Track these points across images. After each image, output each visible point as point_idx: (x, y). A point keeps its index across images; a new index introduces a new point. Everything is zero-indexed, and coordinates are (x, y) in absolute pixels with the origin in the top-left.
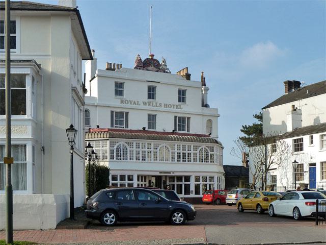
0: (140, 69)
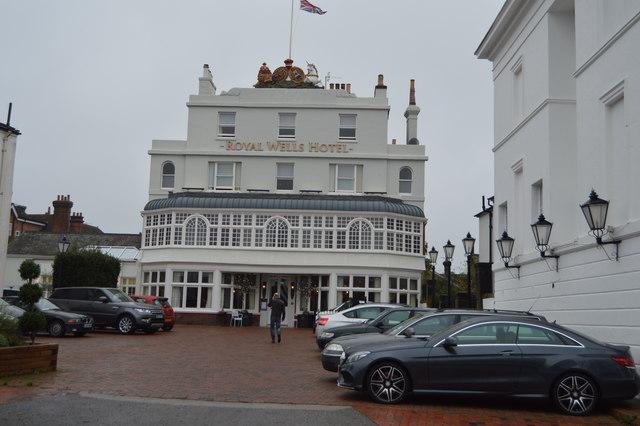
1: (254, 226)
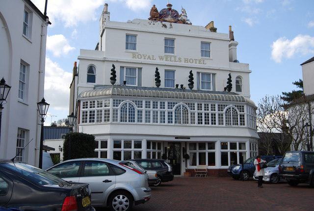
0: (155, 20)
1: (166, 110)
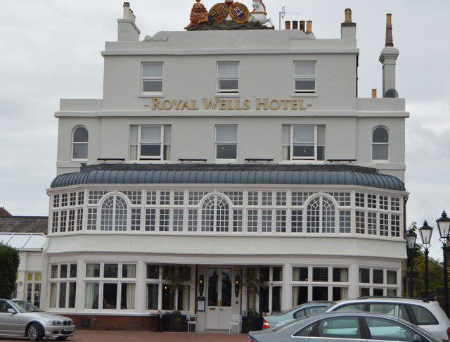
1: (186, 206)
